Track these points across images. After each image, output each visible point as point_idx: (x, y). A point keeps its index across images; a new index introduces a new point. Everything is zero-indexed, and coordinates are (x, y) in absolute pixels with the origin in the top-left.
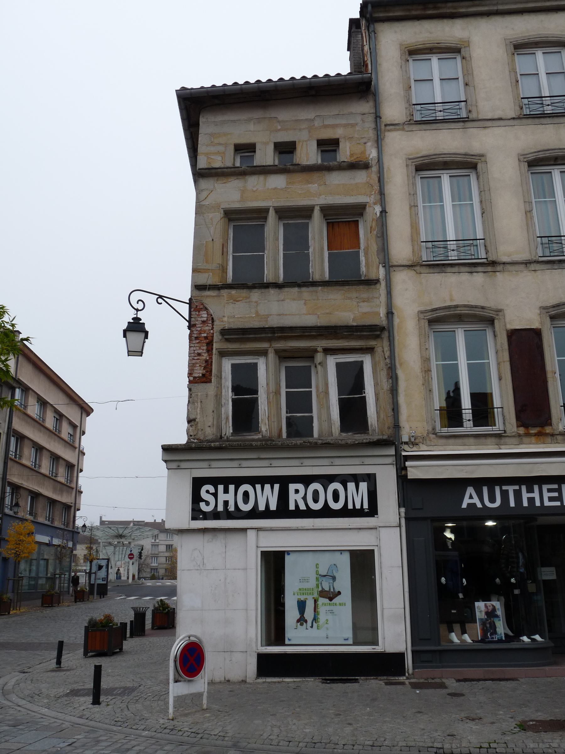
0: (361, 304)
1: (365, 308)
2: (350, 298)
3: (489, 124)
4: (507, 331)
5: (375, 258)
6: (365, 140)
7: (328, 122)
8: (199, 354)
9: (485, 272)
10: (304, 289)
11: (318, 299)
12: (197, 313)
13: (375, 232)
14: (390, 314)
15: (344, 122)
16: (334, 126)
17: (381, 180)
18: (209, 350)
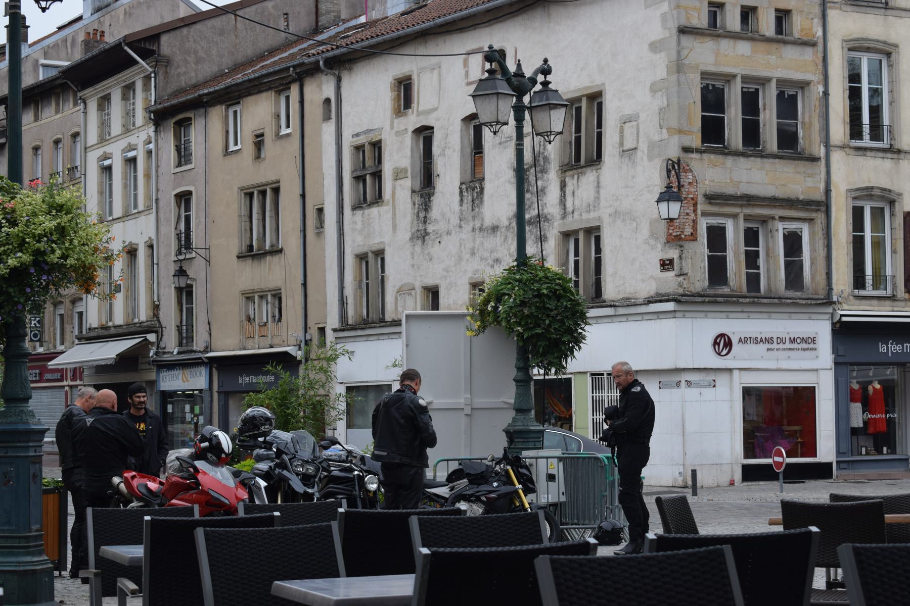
0: (808, 179)
1: (810, 182)
2: (799, 173)
3: (903, 14)
4: (904, 213)
5: (816, 137)
6: (811, 16)
8: (687, 214)
9: (892, 159)
10: (765, 160)
11: (776, 171)
12: (684, 174)
13: (818, 111)
14: (828, 191)
17: (825, 59)
18: (695, 211)
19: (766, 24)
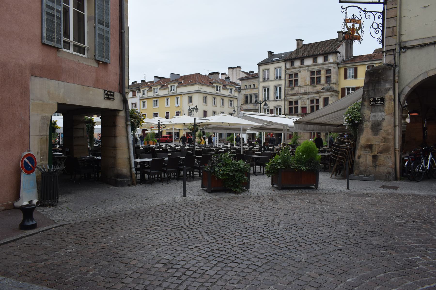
16: (254, 82)
19: (252, 87)
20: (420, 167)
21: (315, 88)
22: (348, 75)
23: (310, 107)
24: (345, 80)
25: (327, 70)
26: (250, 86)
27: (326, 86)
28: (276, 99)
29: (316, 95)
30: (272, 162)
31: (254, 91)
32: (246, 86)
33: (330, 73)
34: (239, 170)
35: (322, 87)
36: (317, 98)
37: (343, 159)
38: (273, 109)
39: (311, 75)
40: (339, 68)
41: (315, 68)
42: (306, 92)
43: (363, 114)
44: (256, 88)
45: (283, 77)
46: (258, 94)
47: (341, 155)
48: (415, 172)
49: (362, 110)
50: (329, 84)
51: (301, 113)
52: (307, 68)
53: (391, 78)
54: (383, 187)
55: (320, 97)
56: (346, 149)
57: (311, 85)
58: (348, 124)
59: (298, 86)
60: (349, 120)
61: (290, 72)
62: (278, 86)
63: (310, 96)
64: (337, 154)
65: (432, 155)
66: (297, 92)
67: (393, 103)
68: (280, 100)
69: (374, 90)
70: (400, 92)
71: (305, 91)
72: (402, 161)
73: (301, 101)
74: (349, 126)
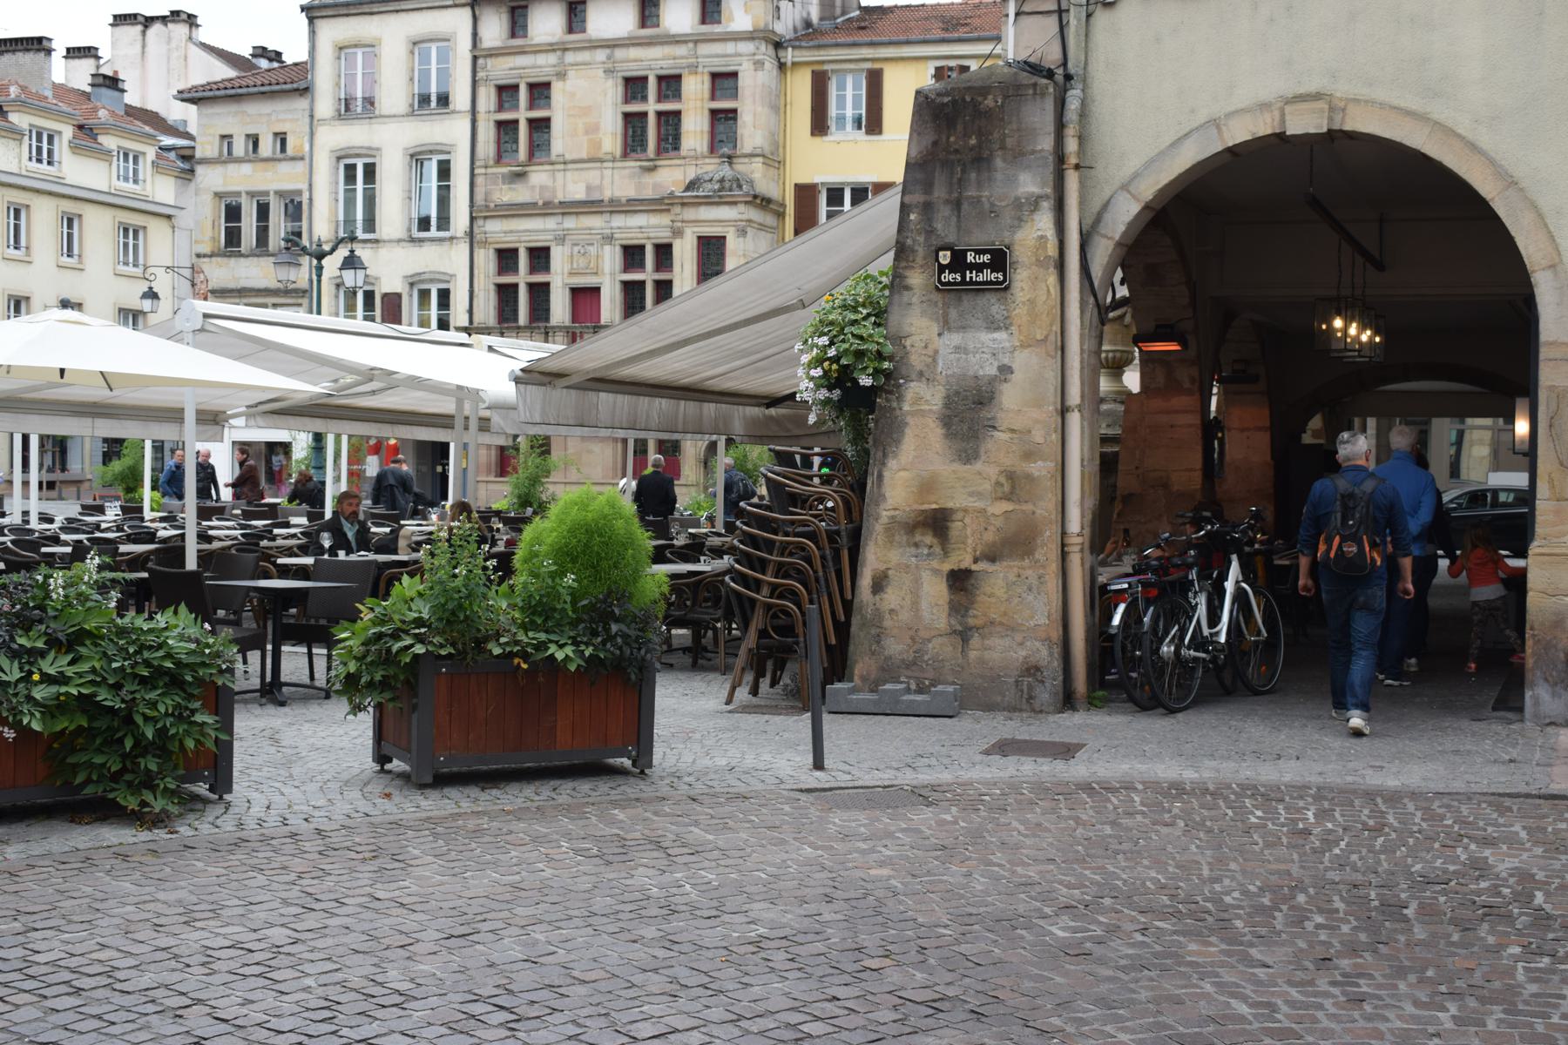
7: (282, 116)
15: (290, 116)
16: (284, 121)
19: (267, 147)
20: (1183, 631)
21: (649, 179)
22: (833, 111)
23: (618, 287)
24: (818, 140)
25: (715, 76)
26: (255, 141)
27: (712, 168)
28: (416, 234)
29: (654, 220)
30: (381, 620)
31: (278, 179)
32: (226, 138)
33: (734, 94)
34: (159, 672)
35: (691, 174)
36: (663, 236)
37: (793, 595)
38: (398, 290)
39: (627, 101)
40: (782, 66)
41: (652, 61)
42: (596, 196)
43: (898, 339)
44: (293, 159)
45: (461, 97)
46: (306, 196)
47: (782, 571)
48: (1160, 665)
49: (894, 318)
50: (730, 157)
51: (567, 322)
52: (601, 55)
53: (1046, 143)
54: (1004, 748)
55: (678, 233)
56: (812, 536)
57: (625, 155)
58: (823, 394)
59: (553, 158)
60: (826, 373)
61: (501, 69)
62: (431, 152)
63: (618, 221)
64: (762, 566)
65: (1243, 566)
66: (548, 196)
67: (1052, 279)
68: (441, 240)
69: (957, 205)
70: (1089, 221)
71: (589, 188)
72: (1101, 600)
73: (567, 249)
74: (826, 402)
